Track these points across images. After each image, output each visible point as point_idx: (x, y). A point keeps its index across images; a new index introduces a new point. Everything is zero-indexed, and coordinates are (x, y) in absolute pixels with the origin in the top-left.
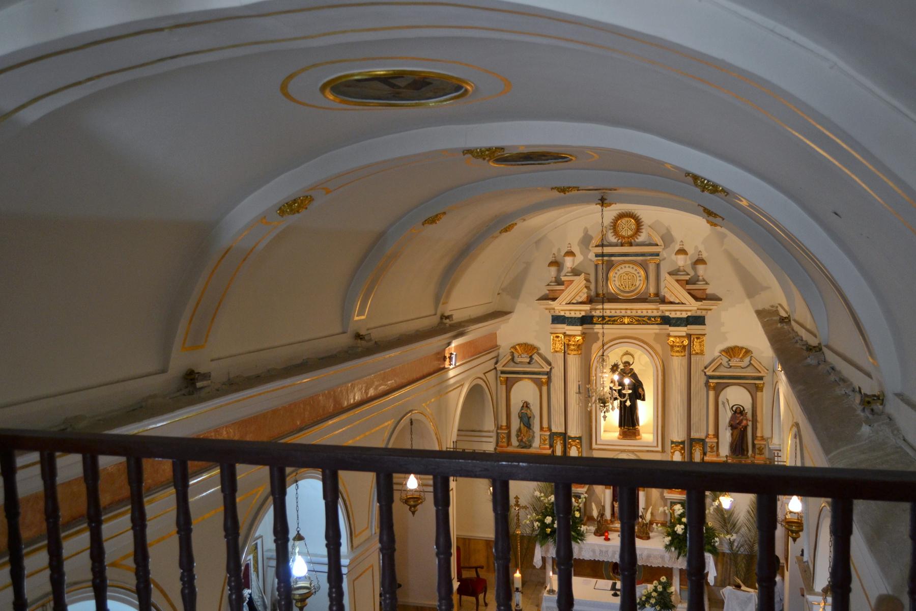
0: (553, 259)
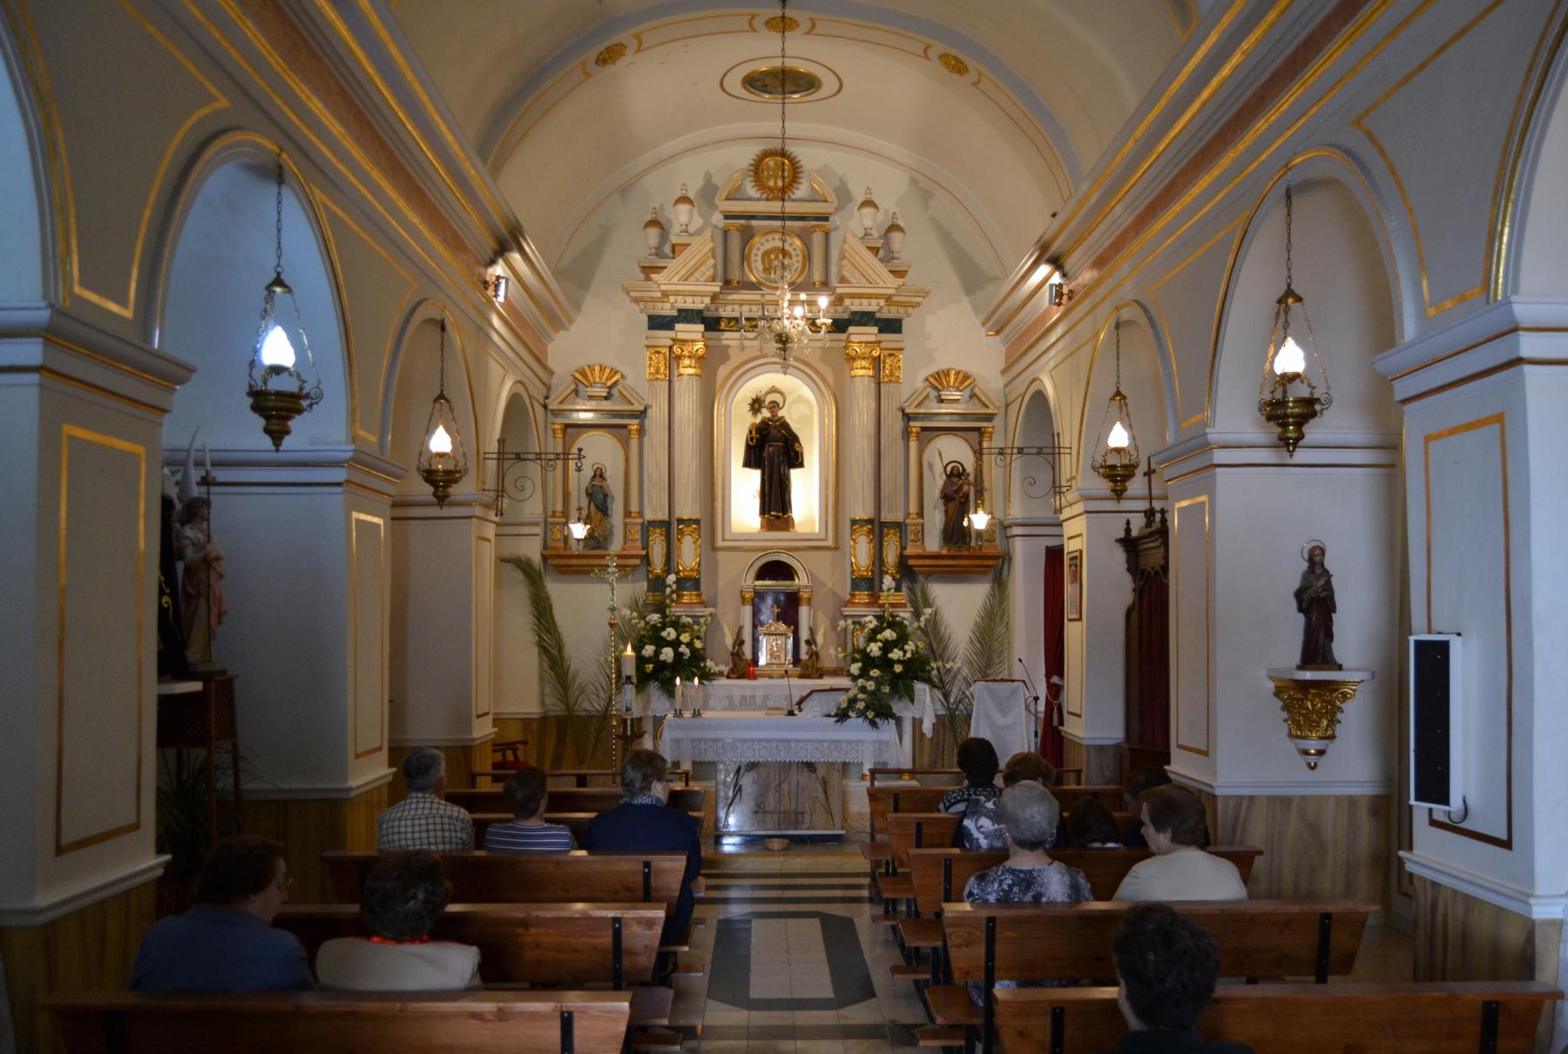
0: (654, 215)
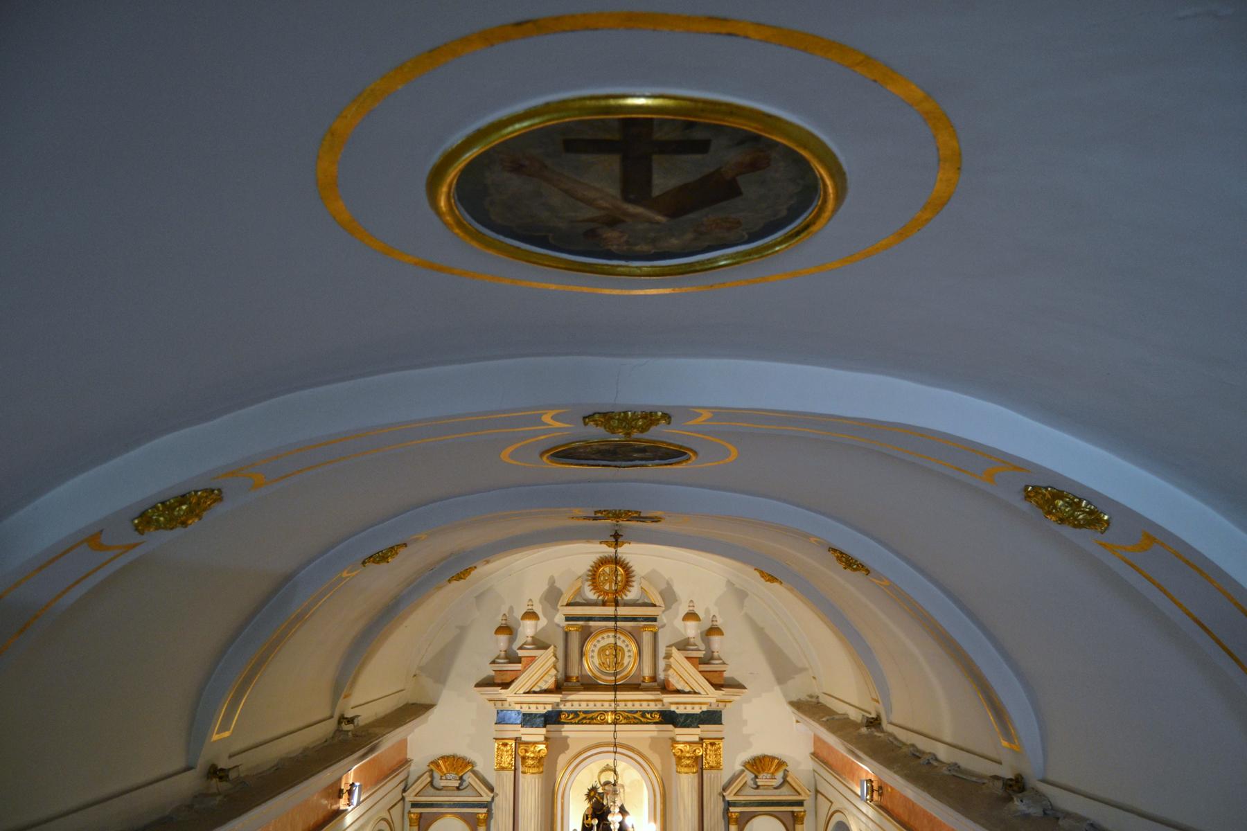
0: (504, 622)
